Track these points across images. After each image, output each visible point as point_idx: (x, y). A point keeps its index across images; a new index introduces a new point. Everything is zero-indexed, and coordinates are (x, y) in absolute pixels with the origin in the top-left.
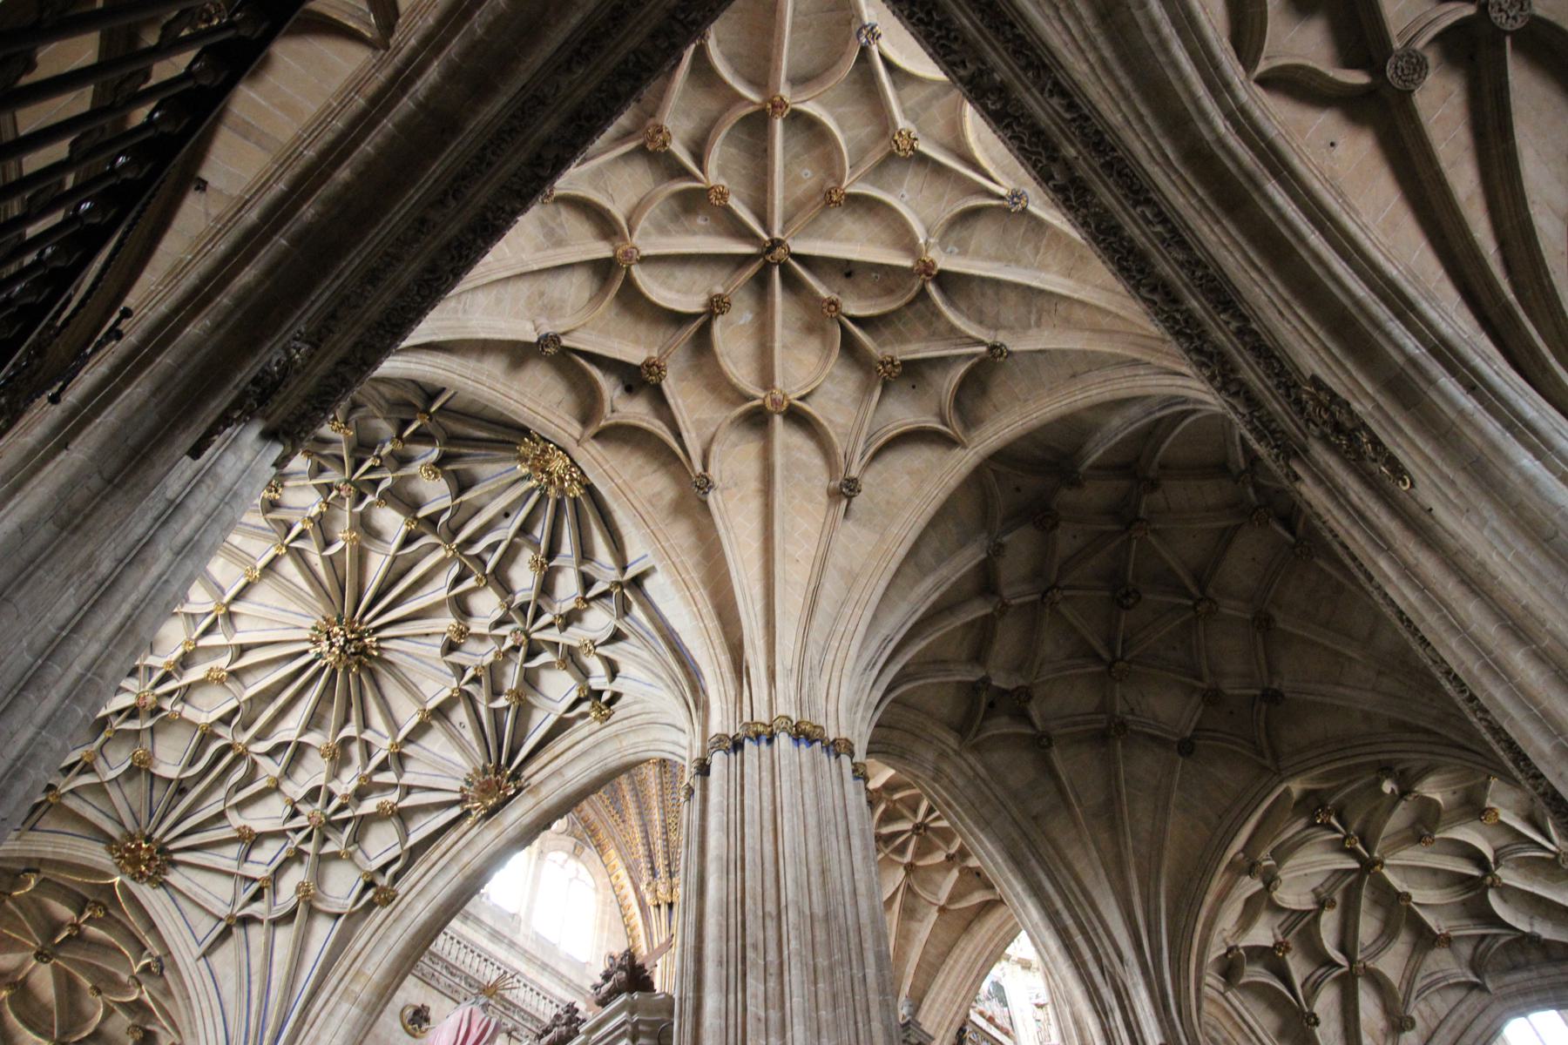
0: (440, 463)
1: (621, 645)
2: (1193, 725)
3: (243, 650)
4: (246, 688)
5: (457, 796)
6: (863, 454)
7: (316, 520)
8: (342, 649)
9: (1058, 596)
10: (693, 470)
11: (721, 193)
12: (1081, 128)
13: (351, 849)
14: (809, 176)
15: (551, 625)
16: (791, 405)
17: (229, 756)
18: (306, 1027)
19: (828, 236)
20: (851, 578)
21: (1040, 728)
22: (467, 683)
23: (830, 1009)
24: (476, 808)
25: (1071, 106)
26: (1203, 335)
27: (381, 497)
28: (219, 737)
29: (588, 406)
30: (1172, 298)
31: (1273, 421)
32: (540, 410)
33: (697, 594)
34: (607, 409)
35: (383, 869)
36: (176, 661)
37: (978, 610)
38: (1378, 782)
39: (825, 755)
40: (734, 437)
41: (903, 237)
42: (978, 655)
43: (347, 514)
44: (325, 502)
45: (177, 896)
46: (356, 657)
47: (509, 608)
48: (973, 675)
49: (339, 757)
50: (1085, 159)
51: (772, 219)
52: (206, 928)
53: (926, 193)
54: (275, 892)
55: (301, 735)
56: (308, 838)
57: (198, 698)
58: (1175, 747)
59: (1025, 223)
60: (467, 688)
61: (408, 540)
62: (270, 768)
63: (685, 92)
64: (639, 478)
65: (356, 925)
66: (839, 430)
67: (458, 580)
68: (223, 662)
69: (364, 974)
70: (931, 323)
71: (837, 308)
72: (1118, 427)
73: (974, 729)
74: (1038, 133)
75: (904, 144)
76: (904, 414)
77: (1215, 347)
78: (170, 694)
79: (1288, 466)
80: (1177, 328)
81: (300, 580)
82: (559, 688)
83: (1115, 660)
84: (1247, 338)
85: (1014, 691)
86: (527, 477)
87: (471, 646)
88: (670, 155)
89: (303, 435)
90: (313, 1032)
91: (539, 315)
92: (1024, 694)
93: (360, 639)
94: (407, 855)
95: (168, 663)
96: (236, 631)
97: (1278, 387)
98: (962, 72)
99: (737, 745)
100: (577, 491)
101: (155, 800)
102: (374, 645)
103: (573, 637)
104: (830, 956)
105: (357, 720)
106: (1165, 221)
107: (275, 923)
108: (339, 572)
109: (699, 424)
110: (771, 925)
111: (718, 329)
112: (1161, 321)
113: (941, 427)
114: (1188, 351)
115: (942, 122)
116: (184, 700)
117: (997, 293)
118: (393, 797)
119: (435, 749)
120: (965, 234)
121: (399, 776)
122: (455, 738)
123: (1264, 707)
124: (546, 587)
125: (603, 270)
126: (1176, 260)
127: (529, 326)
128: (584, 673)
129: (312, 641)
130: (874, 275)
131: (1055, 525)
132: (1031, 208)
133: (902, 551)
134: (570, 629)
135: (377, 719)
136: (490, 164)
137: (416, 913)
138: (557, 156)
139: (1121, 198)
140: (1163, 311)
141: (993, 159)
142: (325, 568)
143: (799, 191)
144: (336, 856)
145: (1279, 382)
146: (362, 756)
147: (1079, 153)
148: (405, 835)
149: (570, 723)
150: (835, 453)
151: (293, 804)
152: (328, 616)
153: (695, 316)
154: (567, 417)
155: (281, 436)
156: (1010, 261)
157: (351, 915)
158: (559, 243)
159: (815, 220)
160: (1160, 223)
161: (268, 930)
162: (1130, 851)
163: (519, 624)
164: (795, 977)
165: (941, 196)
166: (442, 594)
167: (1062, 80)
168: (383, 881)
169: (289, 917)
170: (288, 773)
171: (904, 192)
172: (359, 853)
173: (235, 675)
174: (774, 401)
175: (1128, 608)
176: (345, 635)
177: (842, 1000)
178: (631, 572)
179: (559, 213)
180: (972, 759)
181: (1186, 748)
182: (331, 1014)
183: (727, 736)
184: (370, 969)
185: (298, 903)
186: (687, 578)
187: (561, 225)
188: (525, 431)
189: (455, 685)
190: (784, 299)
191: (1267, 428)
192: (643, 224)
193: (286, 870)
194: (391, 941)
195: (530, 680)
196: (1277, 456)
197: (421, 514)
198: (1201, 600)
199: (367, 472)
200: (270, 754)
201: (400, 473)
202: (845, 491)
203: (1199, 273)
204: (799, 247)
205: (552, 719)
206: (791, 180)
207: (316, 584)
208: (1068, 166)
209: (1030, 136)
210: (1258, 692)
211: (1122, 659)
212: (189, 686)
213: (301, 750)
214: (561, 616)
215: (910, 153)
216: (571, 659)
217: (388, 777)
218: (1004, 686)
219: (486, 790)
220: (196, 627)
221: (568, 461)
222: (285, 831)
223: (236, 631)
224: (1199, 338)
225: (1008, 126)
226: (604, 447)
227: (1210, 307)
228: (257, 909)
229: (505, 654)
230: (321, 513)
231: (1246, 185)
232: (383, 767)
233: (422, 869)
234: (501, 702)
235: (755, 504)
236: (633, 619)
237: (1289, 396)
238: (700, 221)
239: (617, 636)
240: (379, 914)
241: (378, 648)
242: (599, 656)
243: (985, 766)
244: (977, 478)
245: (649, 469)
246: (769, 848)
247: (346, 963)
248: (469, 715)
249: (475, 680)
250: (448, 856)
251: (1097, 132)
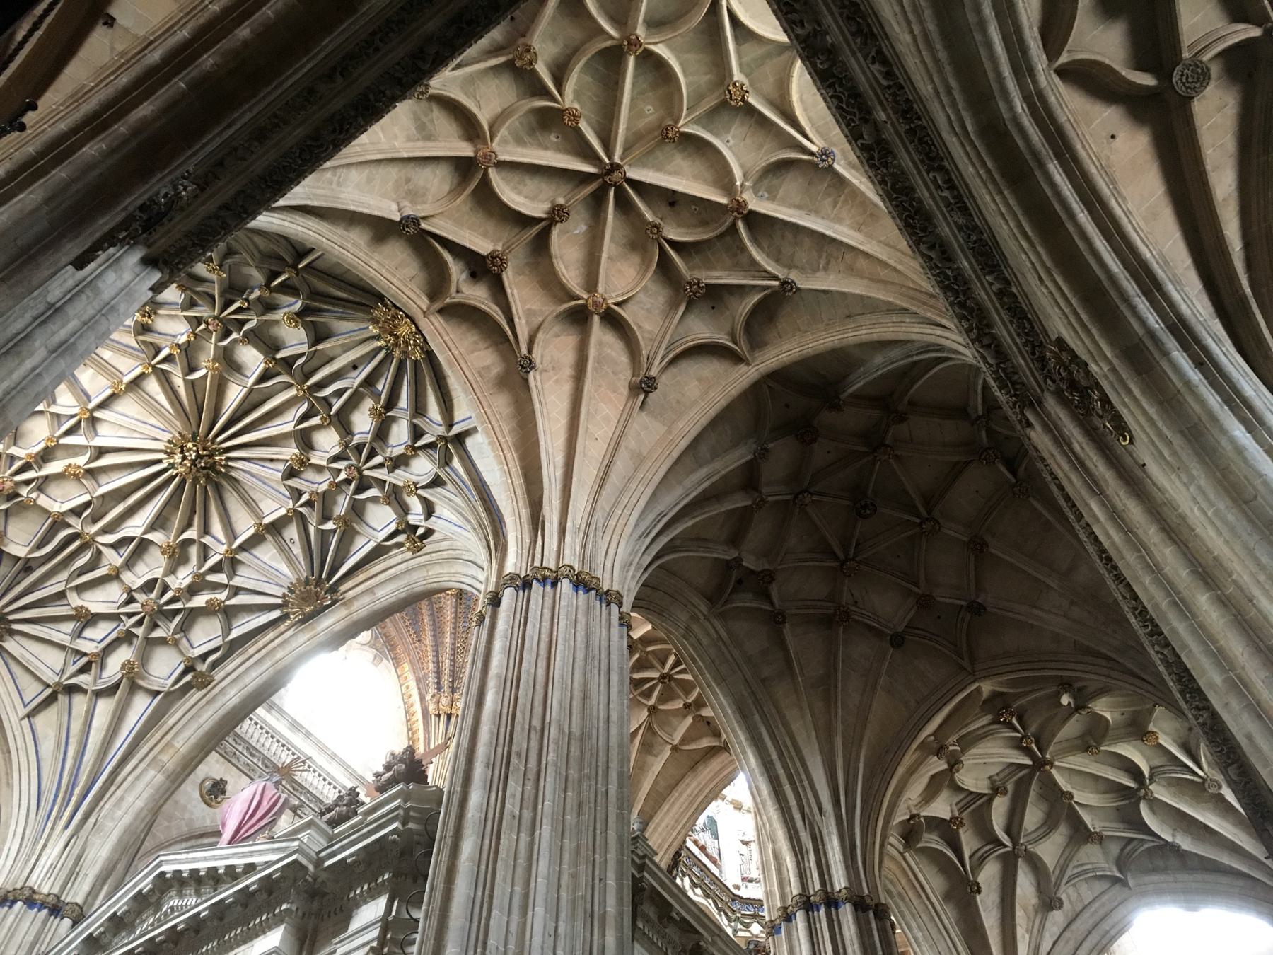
0: (301, 314)
1: (439, 490)
2: (905, 623)
3: (101, 452)
4: (100, 486)
5: (279, 601)
6: (663, 359)
7: (183, 348)
8: (193, 462)
9: (807, 500)
10: (520, 352)
11: (574, 116)
12: (894, 95)
13: (176, 636)
14: (651, 112)
15: (381, 466)
16: (608, 308)
17: (77, 543)
18: (113, 788)
19: (659, 168)
20: (639, 460)
21: (777, 606)
22: (301, 506)
23: (575, 815)
24: (294, 613)
25: (889, 74)
26: (967, 292)
27: (245, 335)
28: (69, 526)
29: (437, 285)
30: (946, 255)
31: (1017, 373)
32: (394, 281)
33: (509, 455)
34: (453, 288)
35: (204, 657)
36: (37, 454)
37: (740, 501)
38: (1058, 695)
39: (598, 602)
40: (557, 329)
41: (723, 178)
42: (735, 540)
43: (213, 346)
44: (193, 332)
45: (11, 662)
46: (205, 472)
47: (347, 447)
48: (729, 555)
49: (177, 556)
50: (892, 124)
51: (615, 146)
52: (33, 691)
53: (748, 141)
54: (102, 667)
55: (145, 533)
56: (139, 623)
57: (54, 489)
58: (889, 638)
59: (829, 179)
60: (300, 509)
61: (264, 377)
62: (113, 559)
63: (554, 18)
64: (472, 352)
65: (171, 704)
66: (647, 335)
67: (305, 417)
68: (81, 460)
69: (173, 746)
70: (735, 255)
71: (658, 231)
72: (879, 363)
73: (723, 601)
74: (856, 95)
75: (736, 94)
76: (701, 330)
77: (977, 304)
78: (27, 483)
79: (1022, 413)
80: (947, 282)
81: (162, 398)
82: (381, 519)
83: (847, 559)
84: (1005, 299)
85: (762, 572)
86: (377, 337)
87: (310, 475)
88: (534, 73)
89: (181, 266)
90: (119, 793)
91: (404, 198)
92: (769, 577)
93: (211, 456)
94: (227, 647)
95: (29, 455)
96: (97, 435)
97: (1025, 345)
98: (799, 31)
99: (526, 585)
100: (418, 355)
102: (223, 463)
103: (399, 477)
104: (581, 770)
105: (199, 526)
106: (952, 187)
107: (98, 694)
108: (198, 396)
109: (530, 313)
110: (535, 737)
111: (555, 233)
112: (934, 276)
113: (730, 344)
114: (952, 304)
115: (772, 80)
116: (40, 489)
117: (795, 237)
118: (222, 596)
119: (265, 559)
120: (775, 182)
121: (230, 578)
122: (284, 551)
123: (968, 616)
124: (381, 433)
125: (464, 168)
126: (955, 222)
127: (394, 207)
128: (404, 510)
129: (166, 452)
130: (694, 207)
131: (814, 440)
132: (836, 166)
133: (684, 444)
134: (397, 471)
135: (217, 527)
136: (377, 49)
137: (228, 697)
138: (437, 53)
139: (918, 163)
140: (937, 267)
141: (810, 119)
142: (186, 390)
143: (641, 124)
144: (162, 641)
145: (1027, 341)
146: (199, 557)
147: (889, 117)
148: (228, 629)
149: (390, 548)
150: (640, 355)
151: (130, 591)
152: (185, 432)
153: (539, 220)
154: (418, 291)
155: (161, 265)
156: (810, 211)
157: (168, 694)
158: (429, 137)
159: (651, 152)
160: (948, 189)
161: (90, 699)
162: (839, 718)
163: (354, 462)
164: (550, 783)
165: (761, 146)
166: (290, 427)
167: (885, 50)
168: (202, 667)
169: (111, 690)
170: (129, 564)
171: (730, 138)
172: (184, 641)
173: (91, 473)
174: (594, 302)
175: (864, 517)
176: (197, 451)
177: (586, 809)
178: (456, 430)
179: (432, 111)
180: (717, 624)
181: (897, 641)
182: (137, 778)
183: (518, 575)
184: (178, 743)
185: (121, 680)
186: (502, 441)
187: (432, 121)
188: (380, 298)
189: (291, 506)
190: (615, 216)
191: (1009, 379)
192: (503, 132)
193: (114, 650)
194: (201, 720)
195: (357, 510)
196: (1014, 404)
197: (279, 356)
198: (927, 519)
199: (234, 312)
200: (115, 546)
201: (264, 318)
202: (644, 387)
203: (974, 238)
204: (633, 174)
205: (372, 544)
206: (635, 113)
207: (176, 402)
208: (877, 128)
209: (849, 97)
210: (964, 603)
211: (853, 559)
212: (47, 478)
213: (143, 546)
214: (391, 459)
215: (741, 103)
216: (395, 497)
217: (221, 578)
218: (752, 568)
219: (305, 598)
220: (60, 426)
221: (414, 329)
222: (119, 614)
223: (97, 435)
224: (964, 295)
225: (831, 86)
226: (446, 321)
227: (977, 268)
228: (83, 680)
229: (339, 485)
230: (188, 342)
231: (1031, 163)
232: (216, 569)
233: (238, 661)
234: (330, 526)
235: (567, 388)
236: (451, 469)
237: (1033, 354)
238: (553, 138)
239: (436, 482)
240: (195, 696)
241: (226, 466)
242: (420, 497)
243: (729, 632)
244: (755, 392)
245: (482, 345)
246: (541, 673)
247: (158, 736)
248: (299, 533)
249: (309, 504)
250: (264, 651)
251: (908, 100)
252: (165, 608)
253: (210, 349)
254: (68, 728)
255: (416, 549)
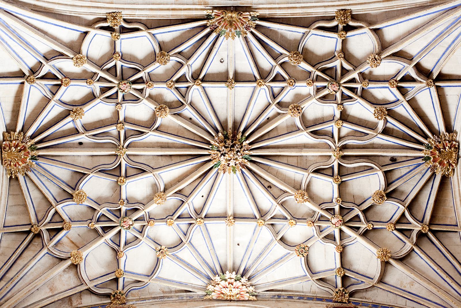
0: (71, 197)
28: (339, 165)
35: (334, 30)
65: (376, 16)
78: (330, 210)
101: (408, 170)
124: (92, 97)
178: (21, 81)
195: (152, 58)
228: (414, 74)
240: (356, 10)
252: (328, 79)
253: (153, 208)
254: (444, 54)
255: (114, 16)
